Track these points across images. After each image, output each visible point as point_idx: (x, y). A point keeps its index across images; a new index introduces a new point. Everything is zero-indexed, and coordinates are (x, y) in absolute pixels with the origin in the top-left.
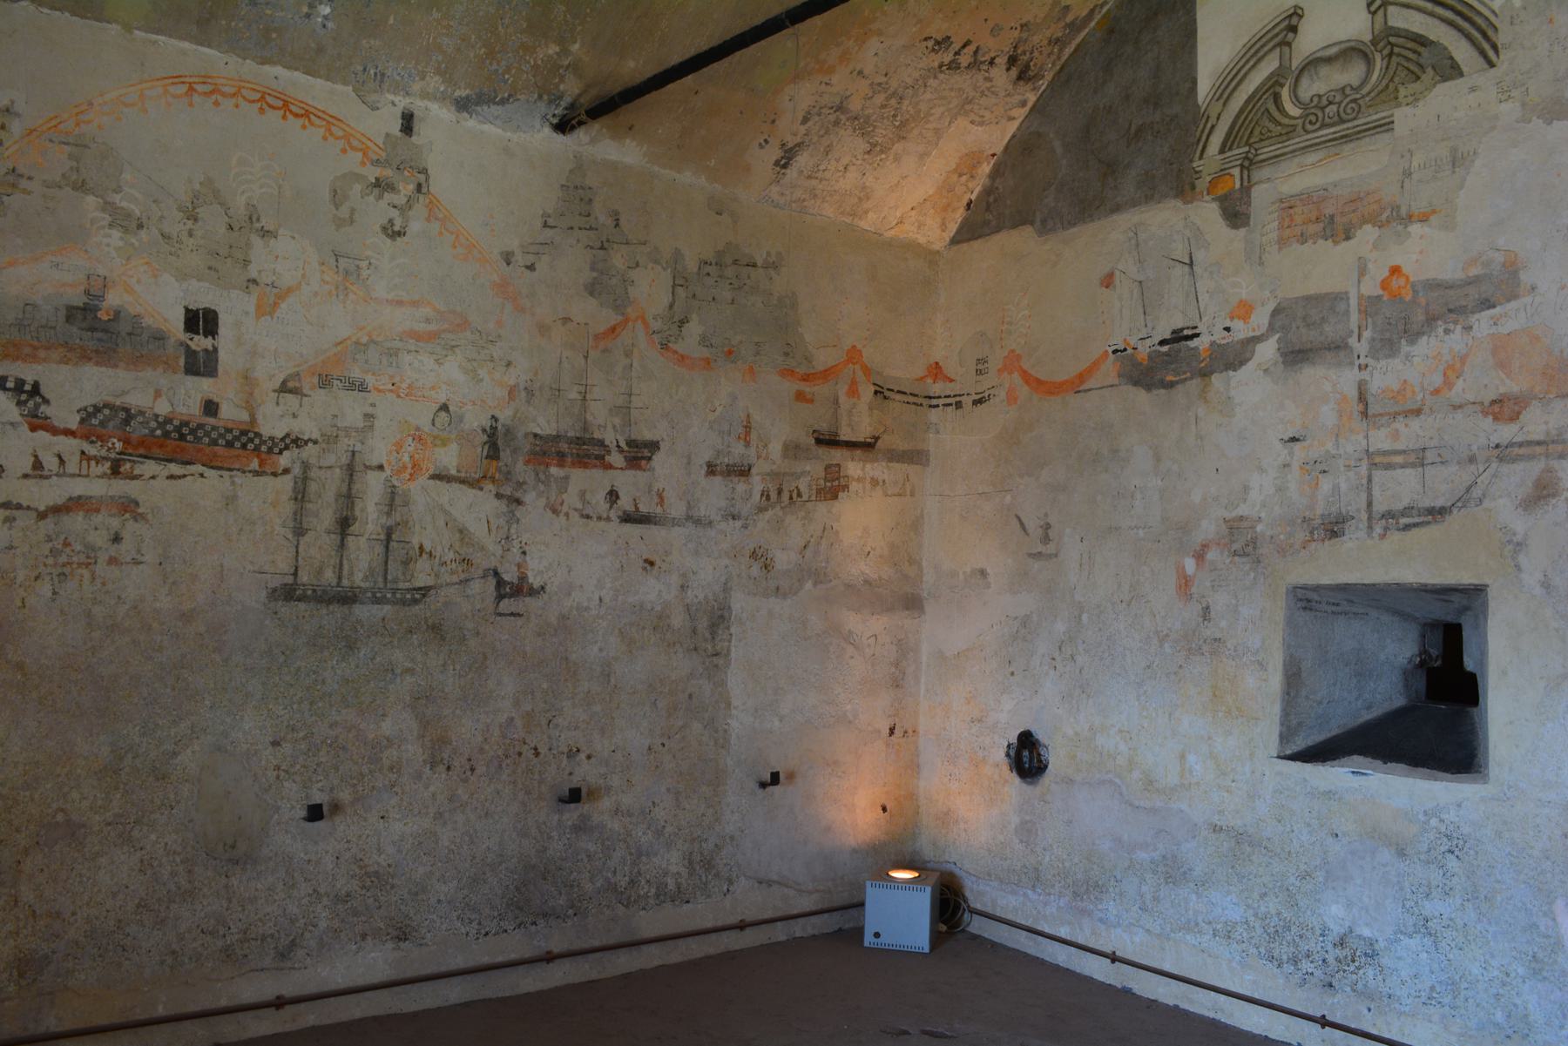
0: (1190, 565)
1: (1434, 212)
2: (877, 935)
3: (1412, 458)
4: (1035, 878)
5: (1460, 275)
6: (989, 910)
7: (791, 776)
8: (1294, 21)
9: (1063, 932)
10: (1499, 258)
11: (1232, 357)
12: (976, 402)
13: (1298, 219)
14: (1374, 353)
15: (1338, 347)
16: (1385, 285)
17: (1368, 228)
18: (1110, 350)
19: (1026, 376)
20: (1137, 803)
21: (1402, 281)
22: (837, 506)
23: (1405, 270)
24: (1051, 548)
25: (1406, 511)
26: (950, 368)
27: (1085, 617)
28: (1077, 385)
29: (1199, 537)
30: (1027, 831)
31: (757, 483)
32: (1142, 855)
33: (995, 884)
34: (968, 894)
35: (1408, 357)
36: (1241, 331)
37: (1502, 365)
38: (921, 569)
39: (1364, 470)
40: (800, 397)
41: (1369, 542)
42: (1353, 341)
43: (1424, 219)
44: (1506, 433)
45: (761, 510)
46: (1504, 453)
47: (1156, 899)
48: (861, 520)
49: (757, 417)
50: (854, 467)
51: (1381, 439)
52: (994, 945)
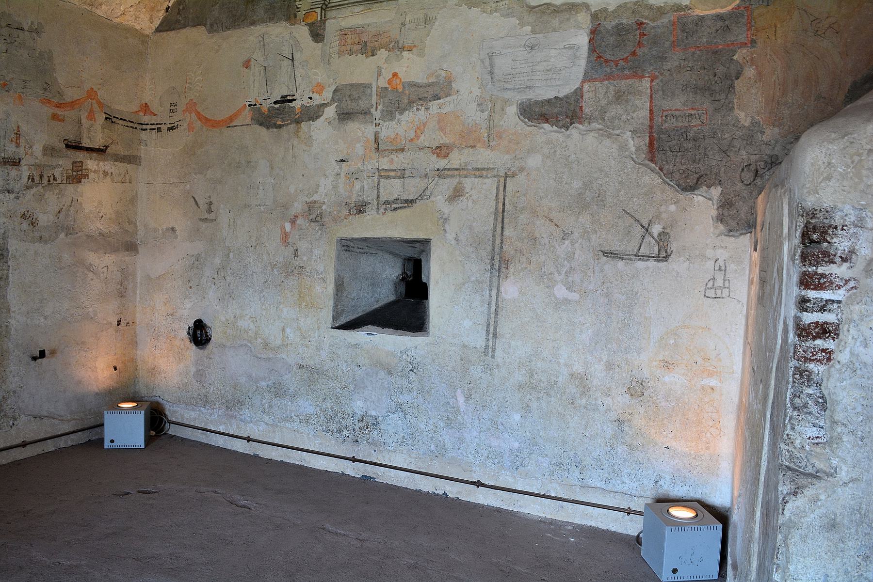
0: (288, 226)
1: (415, 46)
2: (112, 441)
3: (399, 174)
4: (205, 401)
5: (425, 81)
6: (180, 421)
7: (53, 352)
9: (221, 429)
10: (443, 74)
11: (312, 114)
12: (169, 129)
14: (383, 118)
15: (366, 113)
17: (383, 50)
18: (247, 104)
19: (200, 116)
20: (259, 356)
22: (81, 187)
23: (400, 75)
24: (212, 216)
25: (395, 201)
26: (154, 107)
27: (231, 255)
28: (228, 123)
29: (293, 212)
30: (200, 375)
31: (25, 171)
32: (263, 383)
33: (183, 406)
34: (167, 413)
35: (399, 121)
36: (318, 100)
37: (441, 129)
38: (136, 227)
39: (376, 180)
40: (55, 117)
41: (378, 216)
42: (373, 110)
43: (410, 50)
44: (442, 163)
45: (28, 188)
46: (441, 173)
47: (270, 406)
48: (97, 196)
49: (24, 128)
50: (91, 164)
51: (384, 163)
52: (183, 439)
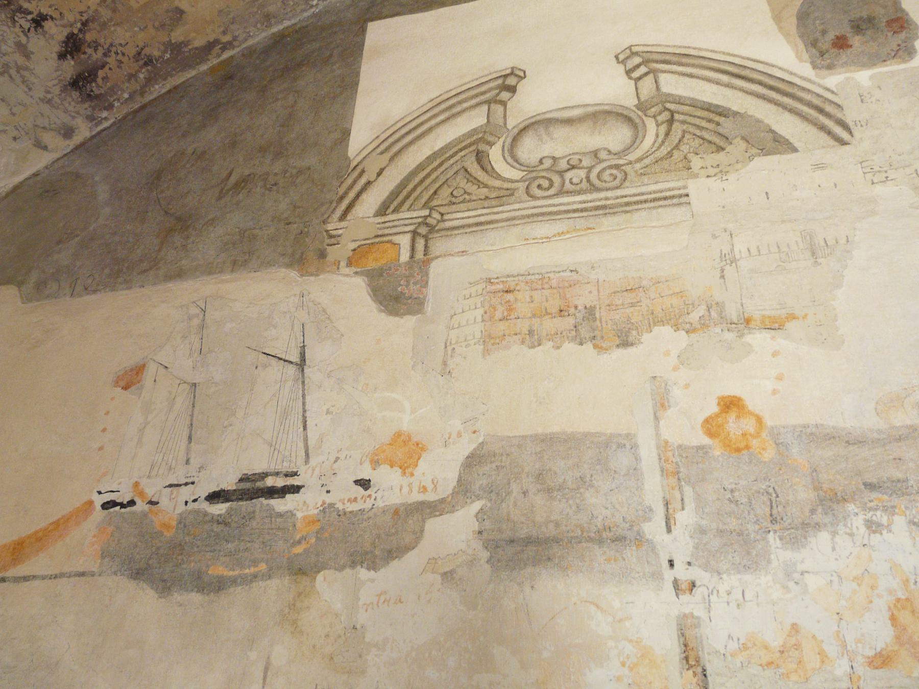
8: (511, 81)
13: (523, 308)
16: (711, 427)
18: (99, 501)
21: (749, 425)
36: (393, 490)
